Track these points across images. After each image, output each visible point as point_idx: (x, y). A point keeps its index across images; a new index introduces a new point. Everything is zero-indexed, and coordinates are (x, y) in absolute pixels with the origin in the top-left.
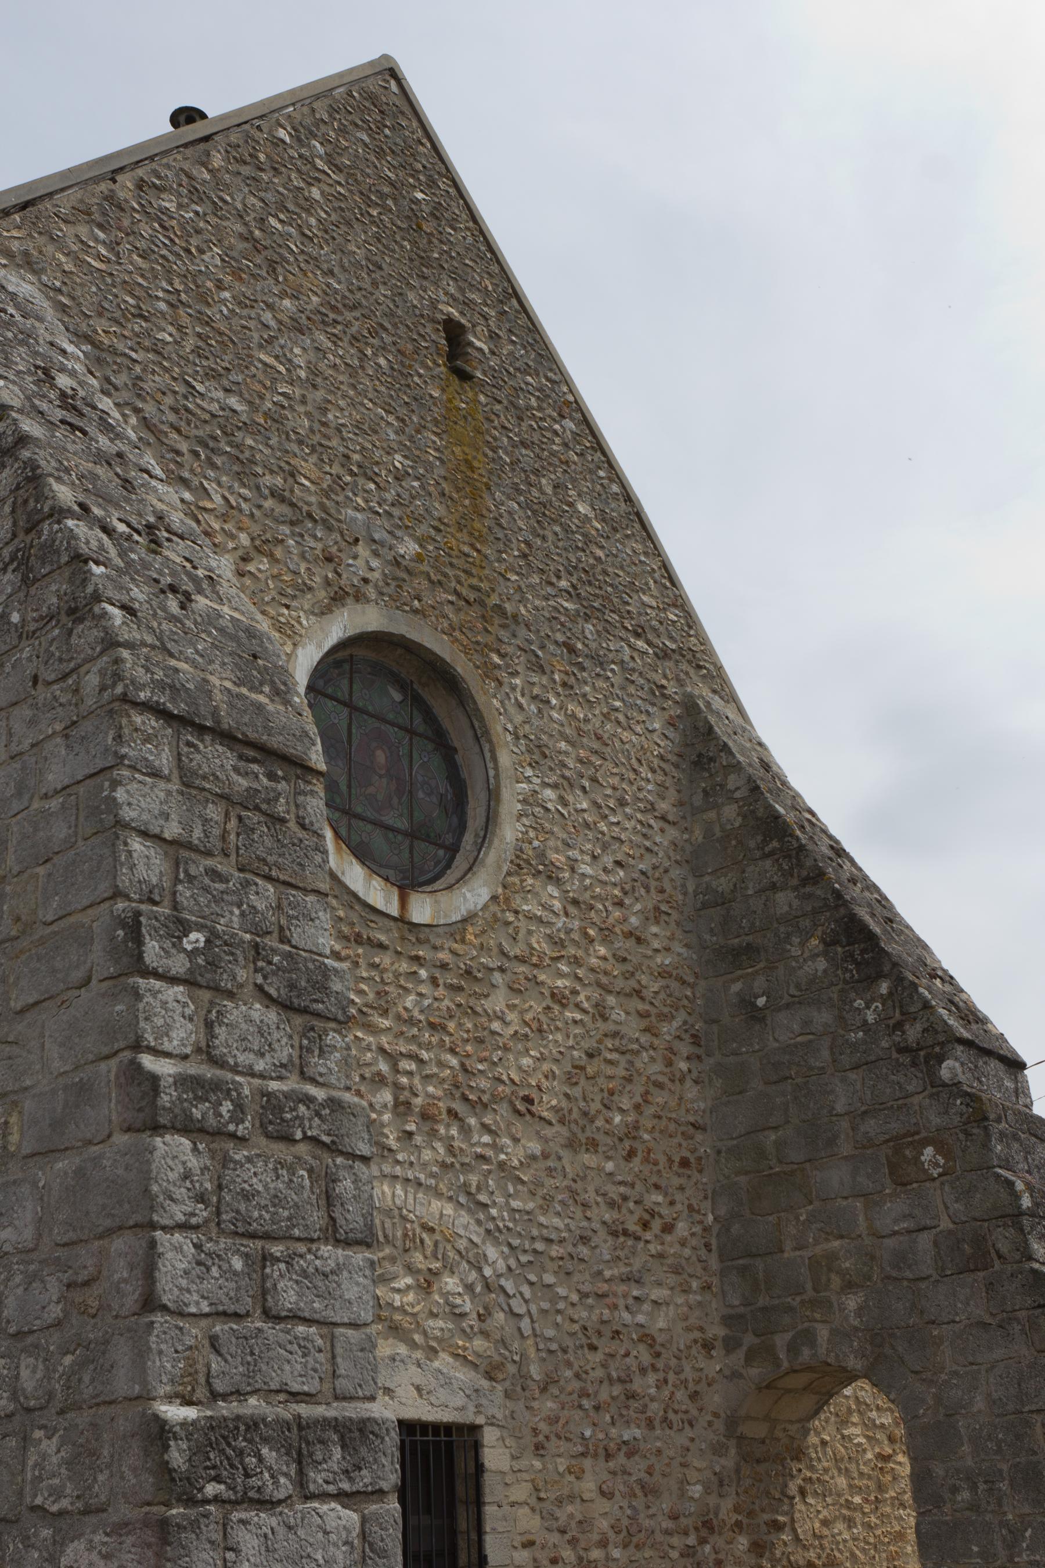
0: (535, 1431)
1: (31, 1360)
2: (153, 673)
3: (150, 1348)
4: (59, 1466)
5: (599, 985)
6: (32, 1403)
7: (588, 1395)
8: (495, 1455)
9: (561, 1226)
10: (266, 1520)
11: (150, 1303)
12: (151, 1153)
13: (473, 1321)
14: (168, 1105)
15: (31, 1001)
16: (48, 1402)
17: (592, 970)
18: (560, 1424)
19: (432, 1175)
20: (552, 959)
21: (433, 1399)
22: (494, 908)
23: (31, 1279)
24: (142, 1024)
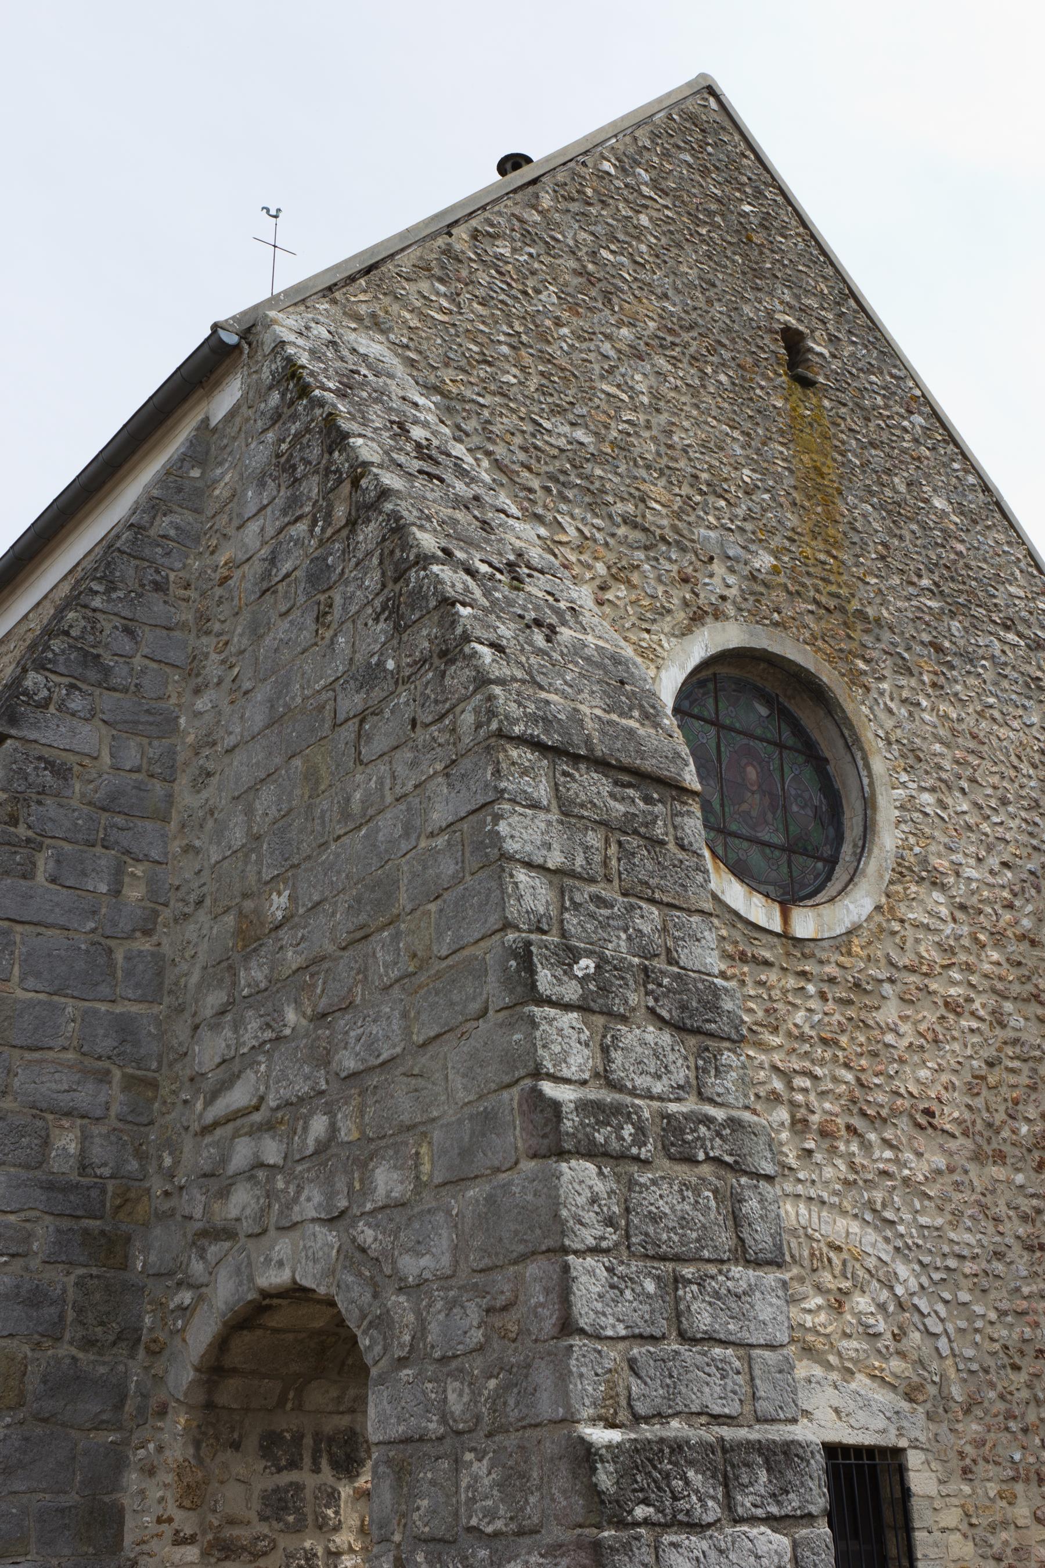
0: (961, 1455)
1: (457, 1384)
2: (525, 707)
3: (570, 1371)
4: (491, 1488)
5: (994, 991)
6: (461, 1426)
7: (1015, 1417)
8: (922, 1479)
9: (974, 1242)
10: (697, 1543)
11: (568, 1326)
12: (558, 1178)
13: (887, 1340)
14: (571, 1130)
15: (432, 1034)
16: (476, 1425)
17: (986, 976)
18: (987, 1447)
19: (835, 1193)
20: (943, 967)
21: (852, 1421)
22: (878, 918)
23: (452, 1304)
24: (540, 1052)
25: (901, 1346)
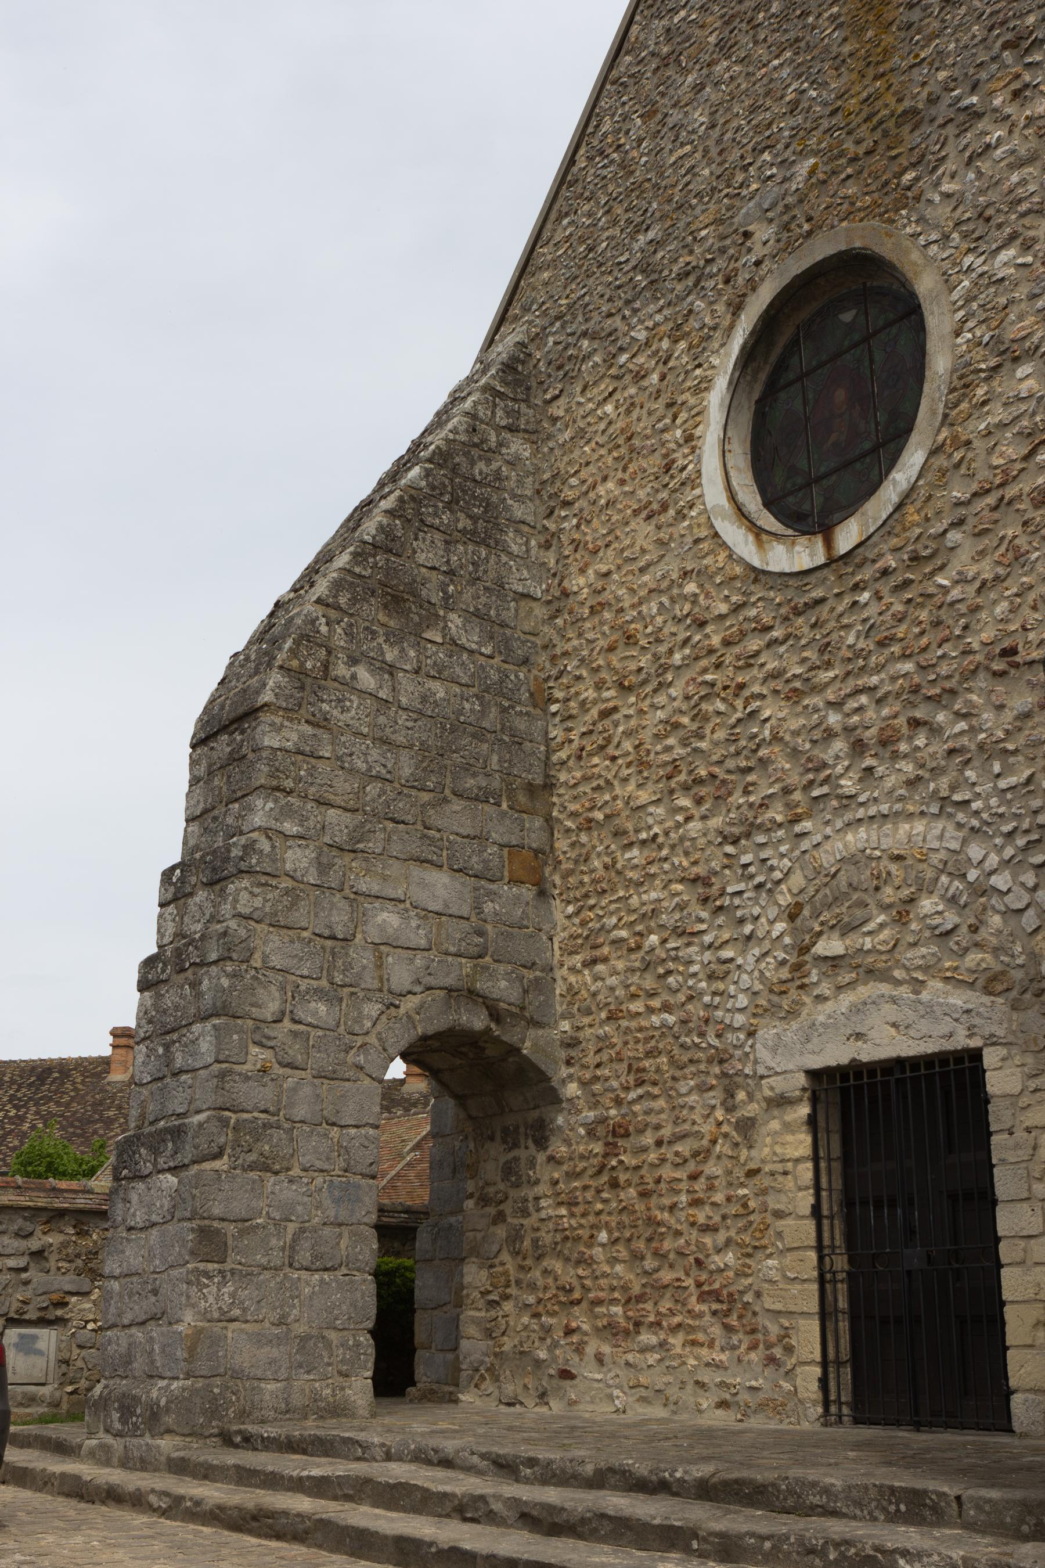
8: (1001, 1079)
10: (141, 1186)
13: (963, 936)
19: (901, 799)
20: (1026, 458)
21: (912, 1033)
22: (941, 461)
25: (978, 938)
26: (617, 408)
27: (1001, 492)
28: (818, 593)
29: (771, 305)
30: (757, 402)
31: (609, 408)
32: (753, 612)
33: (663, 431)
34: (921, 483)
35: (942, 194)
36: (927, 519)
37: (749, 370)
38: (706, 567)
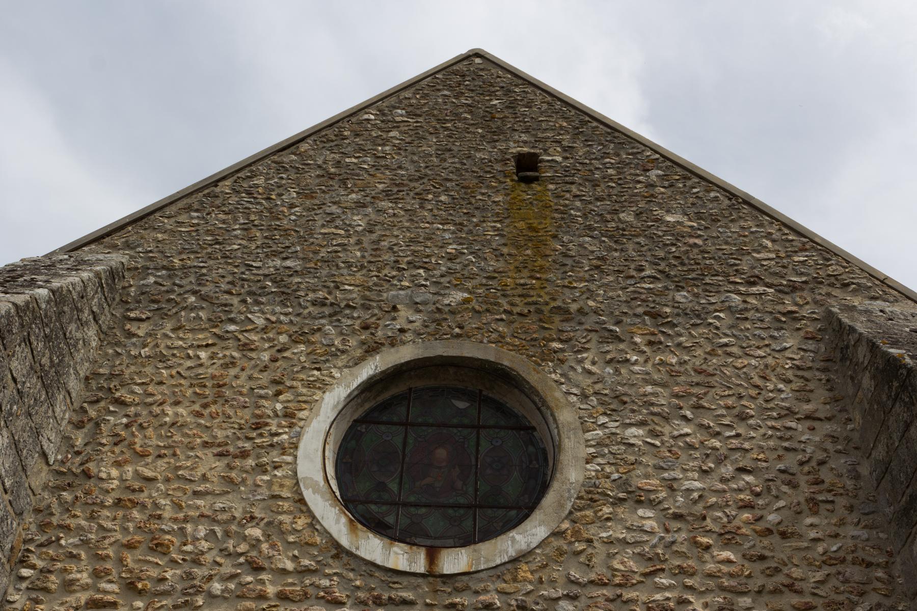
5: (723, 589)
17: (710, 576)
20: (645, 575)
26: (212, 358)
27: (619, 591)
28: (408, 595)
29: (408, 363)
30: (355, 421)
31: (203, 354)
32: (325, 582)
33: (261, 397)
34: (538, 551)
35: (584, 368)
36: (541, 581)
37: (362, 396)
38: (281, 523)
